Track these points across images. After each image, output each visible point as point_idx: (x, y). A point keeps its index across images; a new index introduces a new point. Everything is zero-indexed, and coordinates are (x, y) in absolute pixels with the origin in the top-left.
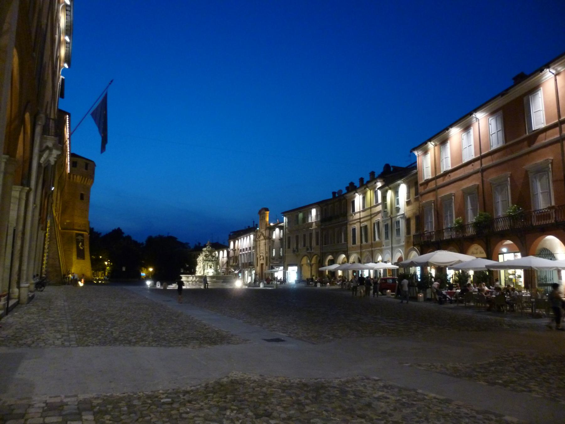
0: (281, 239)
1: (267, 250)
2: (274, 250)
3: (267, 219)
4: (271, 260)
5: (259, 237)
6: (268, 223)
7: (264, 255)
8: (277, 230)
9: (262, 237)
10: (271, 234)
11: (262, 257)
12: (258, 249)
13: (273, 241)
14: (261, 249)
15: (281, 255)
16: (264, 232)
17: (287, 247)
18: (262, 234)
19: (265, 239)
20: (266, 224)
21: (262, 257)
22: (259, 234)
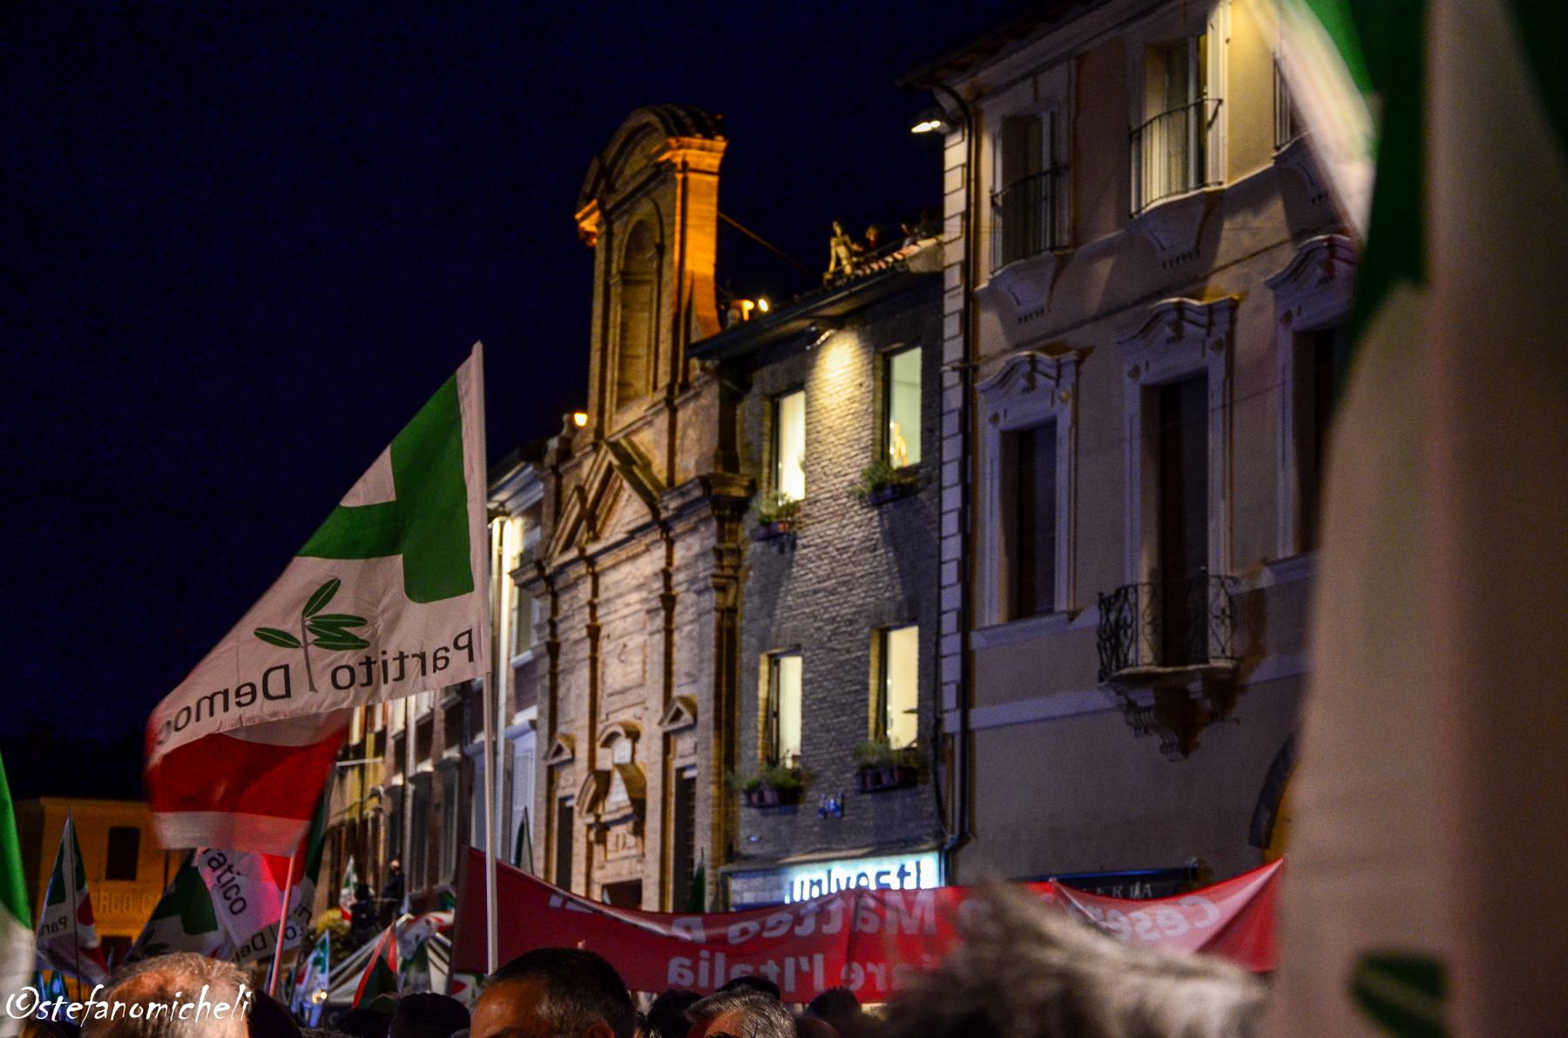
0: (889, 491)
1: (696, 686)
2: (792, 668)
3: (700, 254)
4: (751, 830)
5: (592, 519)
6: (705, 305)
7: (649, 755)
8: (840, 363)
9: (629, 511)
10: (742, 454)
11: (619, 796)
12: (576, 687)
13: (782, 532)
14: (615, 674)
15: (903, 731)
16: (652, 443)
17: (993, 607)
18: (629, 461)
19: (662, 527)
20: (683, 315)
21: (619, 796)
22: (590, 469)
